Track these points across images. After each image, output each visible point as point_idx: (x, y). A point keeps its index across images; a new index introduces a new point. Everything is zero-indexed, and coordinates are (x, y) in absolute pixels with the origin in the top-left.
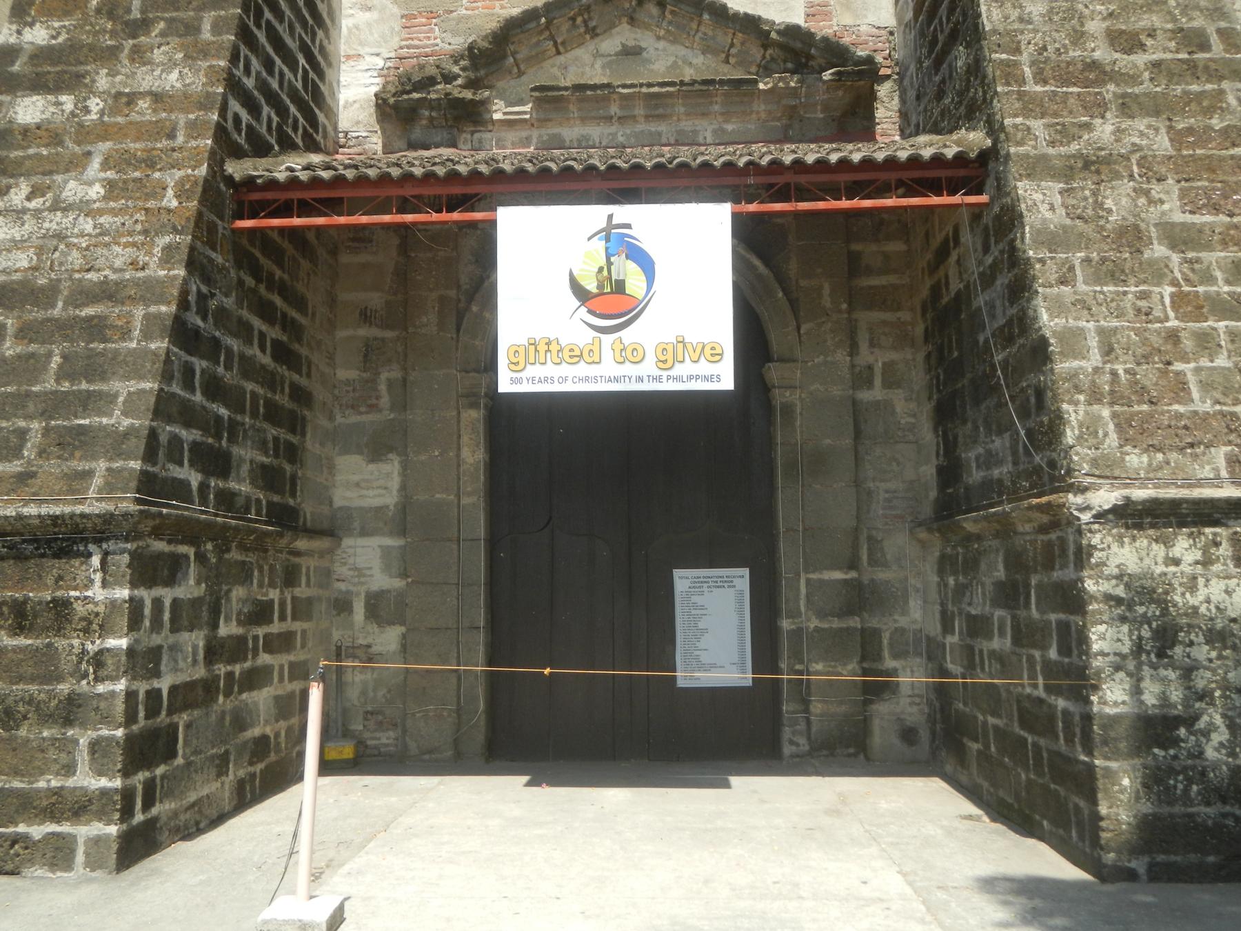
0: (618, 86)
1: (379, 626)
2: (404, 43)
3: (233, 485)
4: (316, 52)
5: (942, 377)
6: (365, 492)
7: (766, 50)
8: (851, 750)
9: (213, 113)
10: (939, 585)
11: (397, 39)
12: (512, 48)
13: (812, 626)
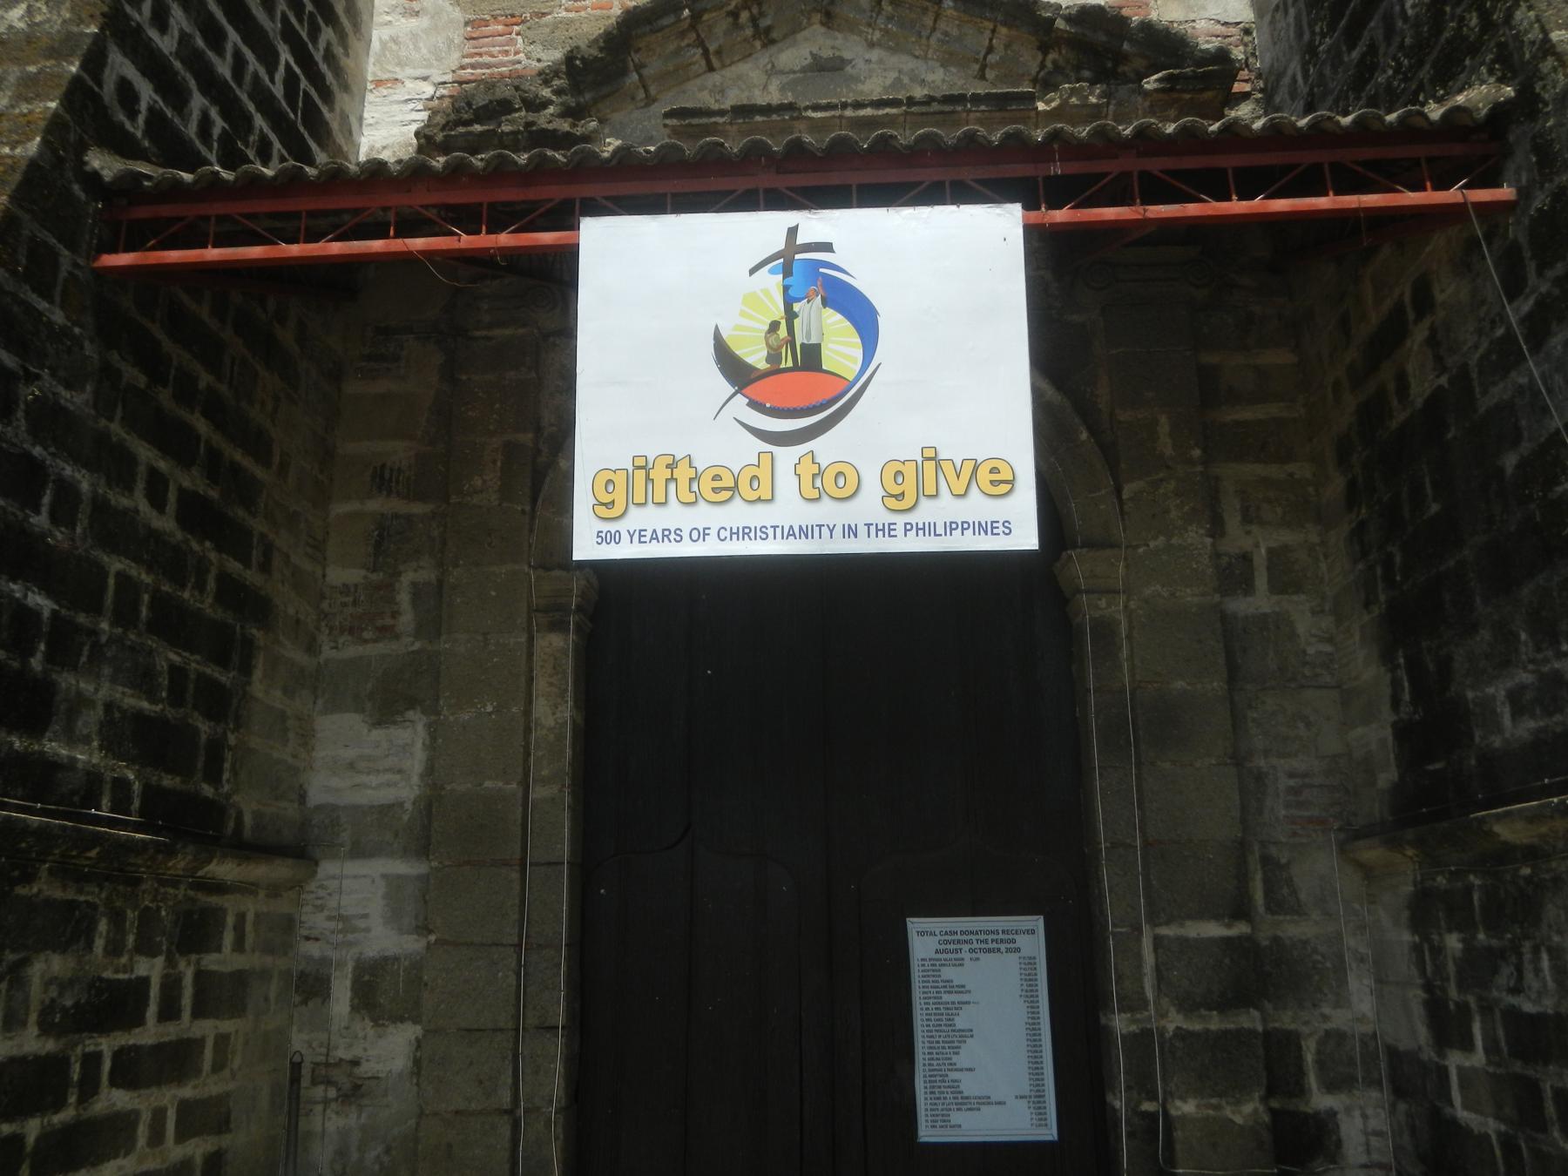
0: (806, 108)
2: (467, 61)
3: (54, 747)
4: (318, 57)
5: (1398, 559)
6: (364, 779)
7: (1045, 54)
9: (72, 63)
10: (1416, 949)
11: (456, 55)
12: (636, 57)
13: (1171, 1027)
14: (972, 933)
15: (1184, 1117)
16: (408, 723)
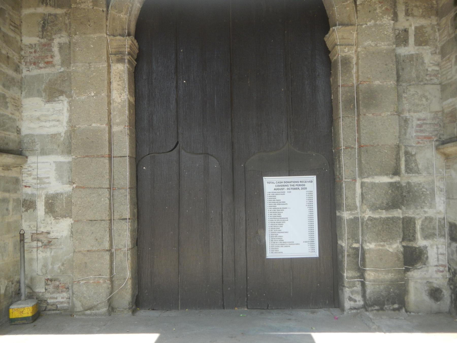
1: (55, 218)
6: (43, 124)
8: (396, 306)
13: (367, 216)
14: (288, 182)
15: (370, 250)
16: (60, 101)
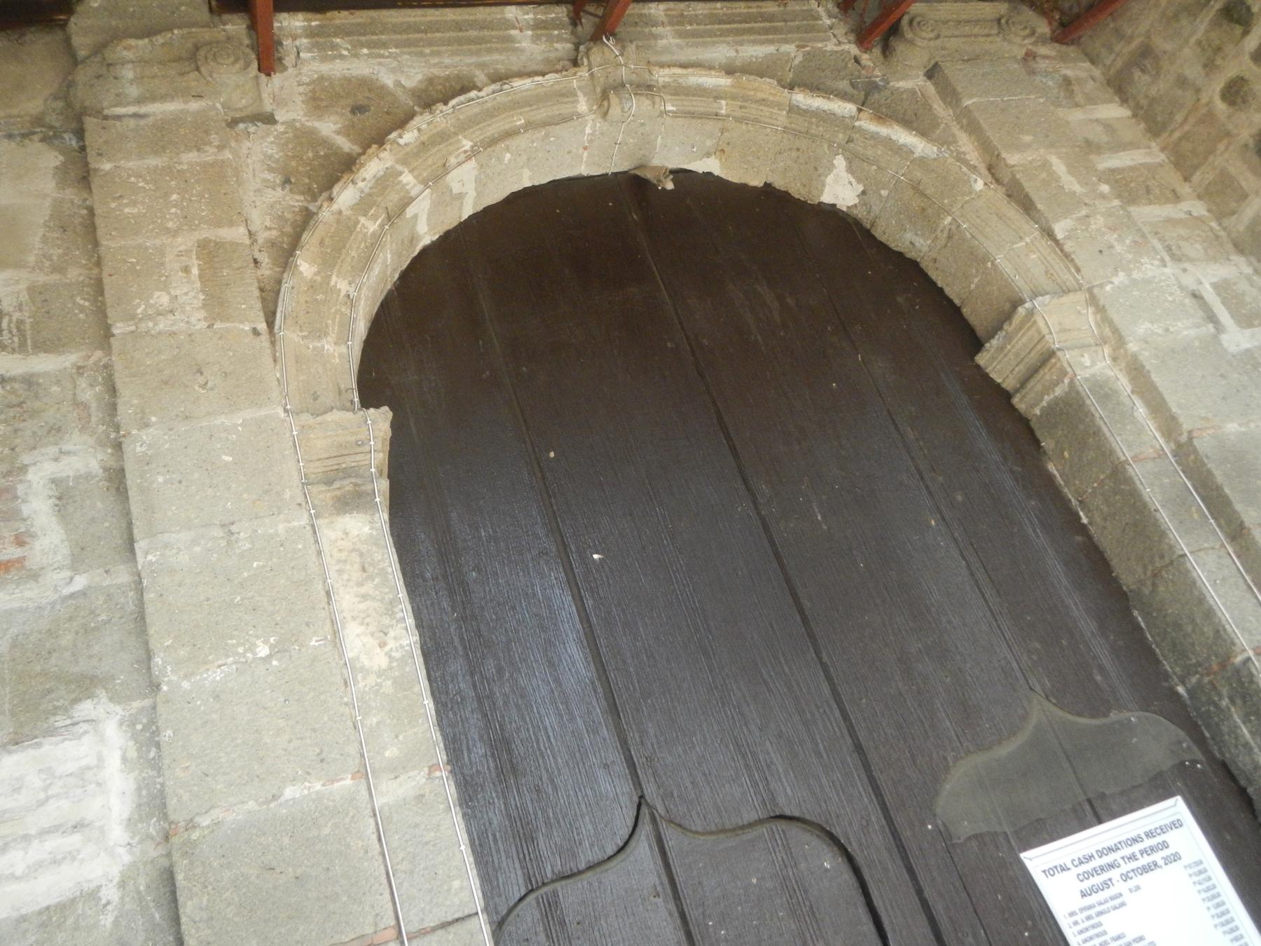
14: (1111, 850)
16: (85, 727)
